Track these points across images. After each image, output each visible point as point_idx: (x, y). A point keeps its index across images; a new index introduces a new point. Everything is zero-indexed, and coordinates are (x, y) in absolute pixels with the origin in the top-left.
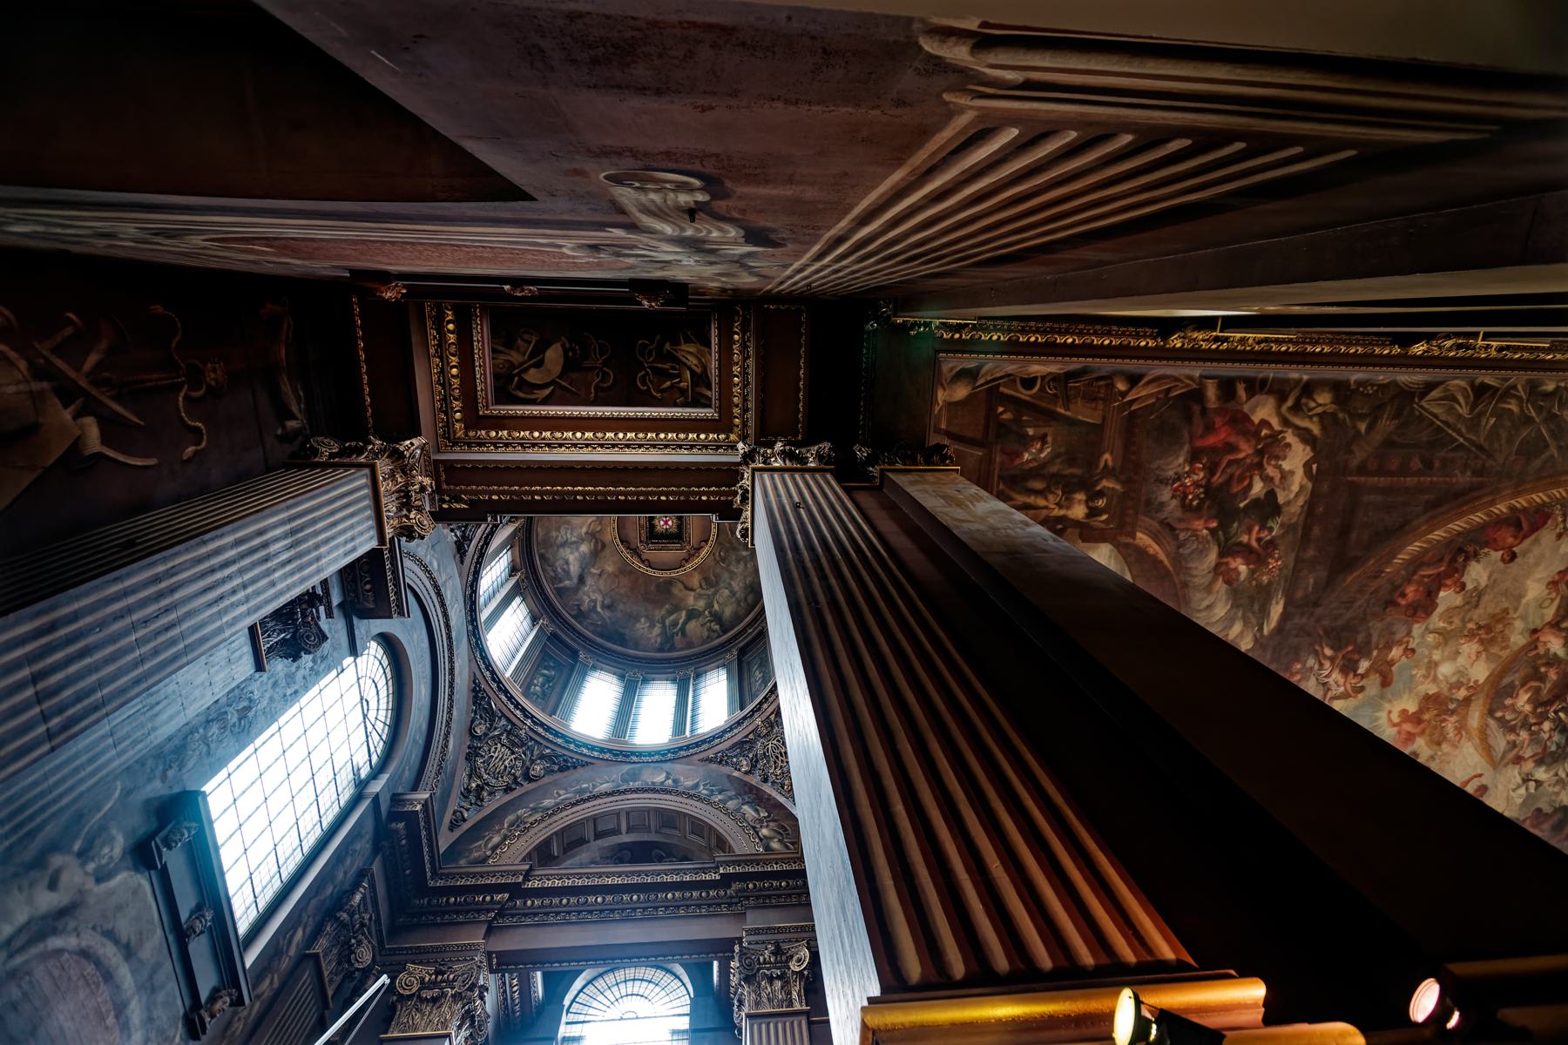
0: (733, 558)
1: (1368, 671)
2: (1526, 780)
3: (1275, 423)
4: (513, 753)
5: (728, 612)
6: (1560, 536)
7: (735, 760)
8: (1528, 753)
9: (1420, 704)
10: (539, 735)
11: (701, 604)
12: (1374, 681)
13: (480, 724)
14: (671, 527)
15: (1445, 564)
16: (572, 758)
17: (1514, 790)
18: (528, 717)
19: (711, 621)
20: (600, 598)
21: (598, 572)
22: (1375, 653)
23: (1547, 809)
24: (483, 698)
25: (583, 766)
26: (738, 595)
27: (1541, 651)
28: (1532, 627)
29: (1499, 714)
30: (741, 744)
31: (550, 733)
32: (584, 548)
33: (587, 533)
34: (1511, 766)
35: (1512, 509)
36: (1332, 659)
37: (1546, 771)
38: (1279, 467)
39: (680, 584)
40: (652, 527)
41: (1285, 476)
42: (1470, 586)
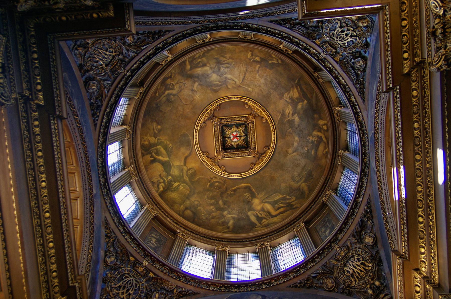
0: (215, 193)
4: (107, 65)
5: (174, 195)
7: (112, 249)
10: (119, 83)
11: (175, 172)
13: (134, 39)
14: (232, 141)
16: (100, 112)
18: (132, 73)
19: (164, 182)
20: (174, 92)
21: (195, 88)
24: (153, 38)
25: (94, 121)
26: (188, 202)
30: (127, 254)
31: (119, 91)
32: (214, 77)
33: (226, 78)
39: (188, 152)
40: (229, 126)
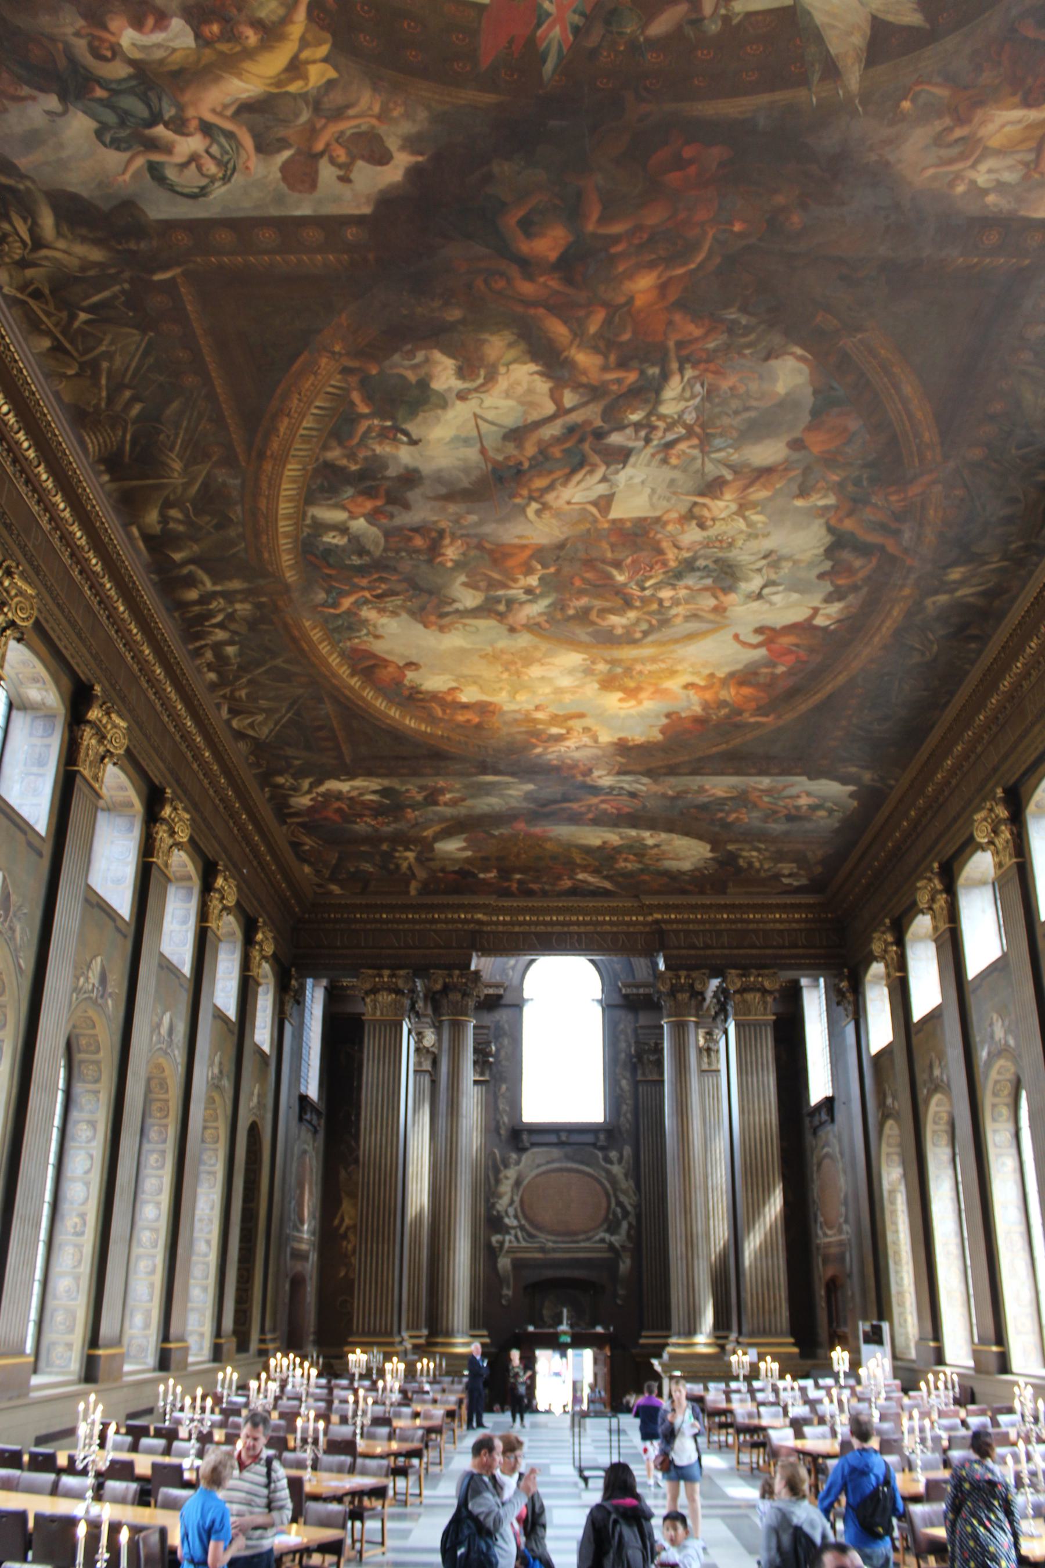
1: (561, 727)
2: (759, 596)
3: (309, 797)
6: (377, 637)
8: (712, 602)
9: (611, 691)
12: (577, 724)
15: (428, 704)
17: (771, 604)
22: (540, 727)
23: (827, 565)
27: (541, 620)
28: (506, 633)
29: (638, 635)
34: (727, 614)
35: (352, 675)
36: (546, 748)
37: (747, 580)
38: (349, 792)
41: (353, 788)
42: (454, 685)
